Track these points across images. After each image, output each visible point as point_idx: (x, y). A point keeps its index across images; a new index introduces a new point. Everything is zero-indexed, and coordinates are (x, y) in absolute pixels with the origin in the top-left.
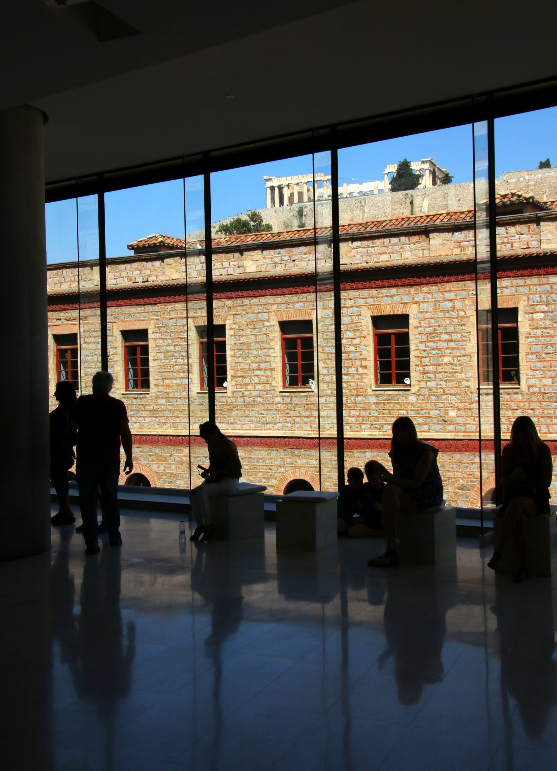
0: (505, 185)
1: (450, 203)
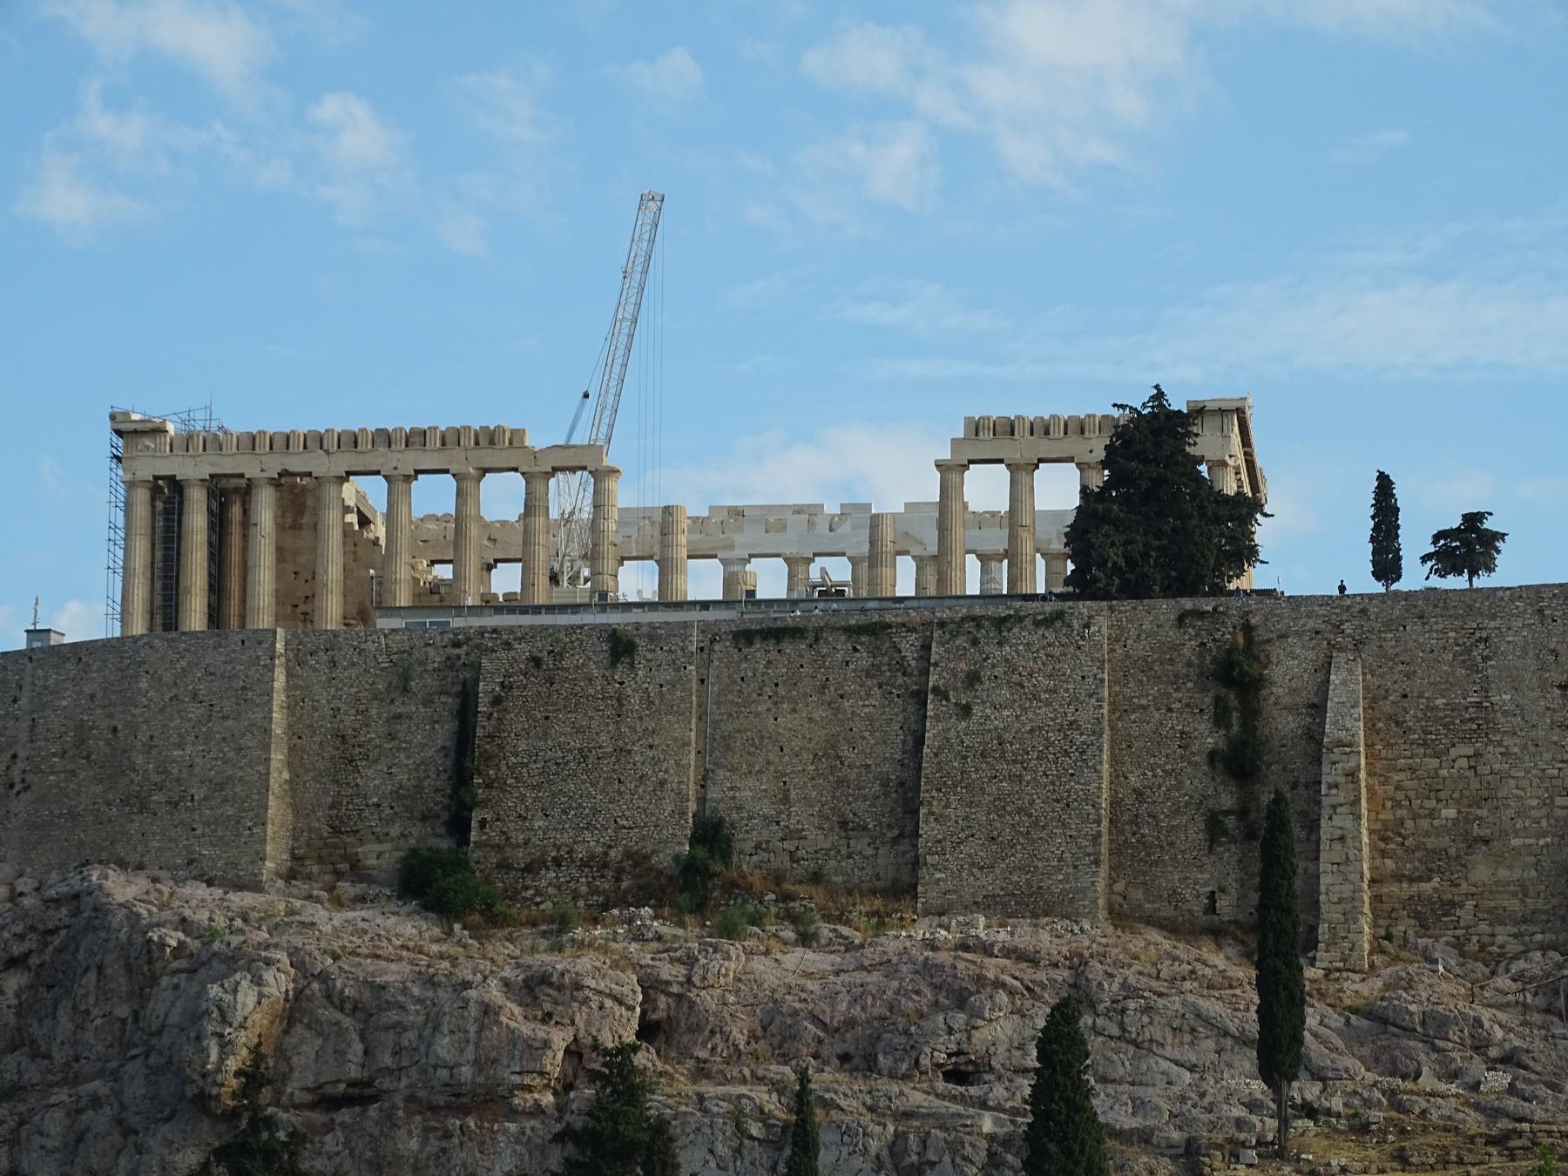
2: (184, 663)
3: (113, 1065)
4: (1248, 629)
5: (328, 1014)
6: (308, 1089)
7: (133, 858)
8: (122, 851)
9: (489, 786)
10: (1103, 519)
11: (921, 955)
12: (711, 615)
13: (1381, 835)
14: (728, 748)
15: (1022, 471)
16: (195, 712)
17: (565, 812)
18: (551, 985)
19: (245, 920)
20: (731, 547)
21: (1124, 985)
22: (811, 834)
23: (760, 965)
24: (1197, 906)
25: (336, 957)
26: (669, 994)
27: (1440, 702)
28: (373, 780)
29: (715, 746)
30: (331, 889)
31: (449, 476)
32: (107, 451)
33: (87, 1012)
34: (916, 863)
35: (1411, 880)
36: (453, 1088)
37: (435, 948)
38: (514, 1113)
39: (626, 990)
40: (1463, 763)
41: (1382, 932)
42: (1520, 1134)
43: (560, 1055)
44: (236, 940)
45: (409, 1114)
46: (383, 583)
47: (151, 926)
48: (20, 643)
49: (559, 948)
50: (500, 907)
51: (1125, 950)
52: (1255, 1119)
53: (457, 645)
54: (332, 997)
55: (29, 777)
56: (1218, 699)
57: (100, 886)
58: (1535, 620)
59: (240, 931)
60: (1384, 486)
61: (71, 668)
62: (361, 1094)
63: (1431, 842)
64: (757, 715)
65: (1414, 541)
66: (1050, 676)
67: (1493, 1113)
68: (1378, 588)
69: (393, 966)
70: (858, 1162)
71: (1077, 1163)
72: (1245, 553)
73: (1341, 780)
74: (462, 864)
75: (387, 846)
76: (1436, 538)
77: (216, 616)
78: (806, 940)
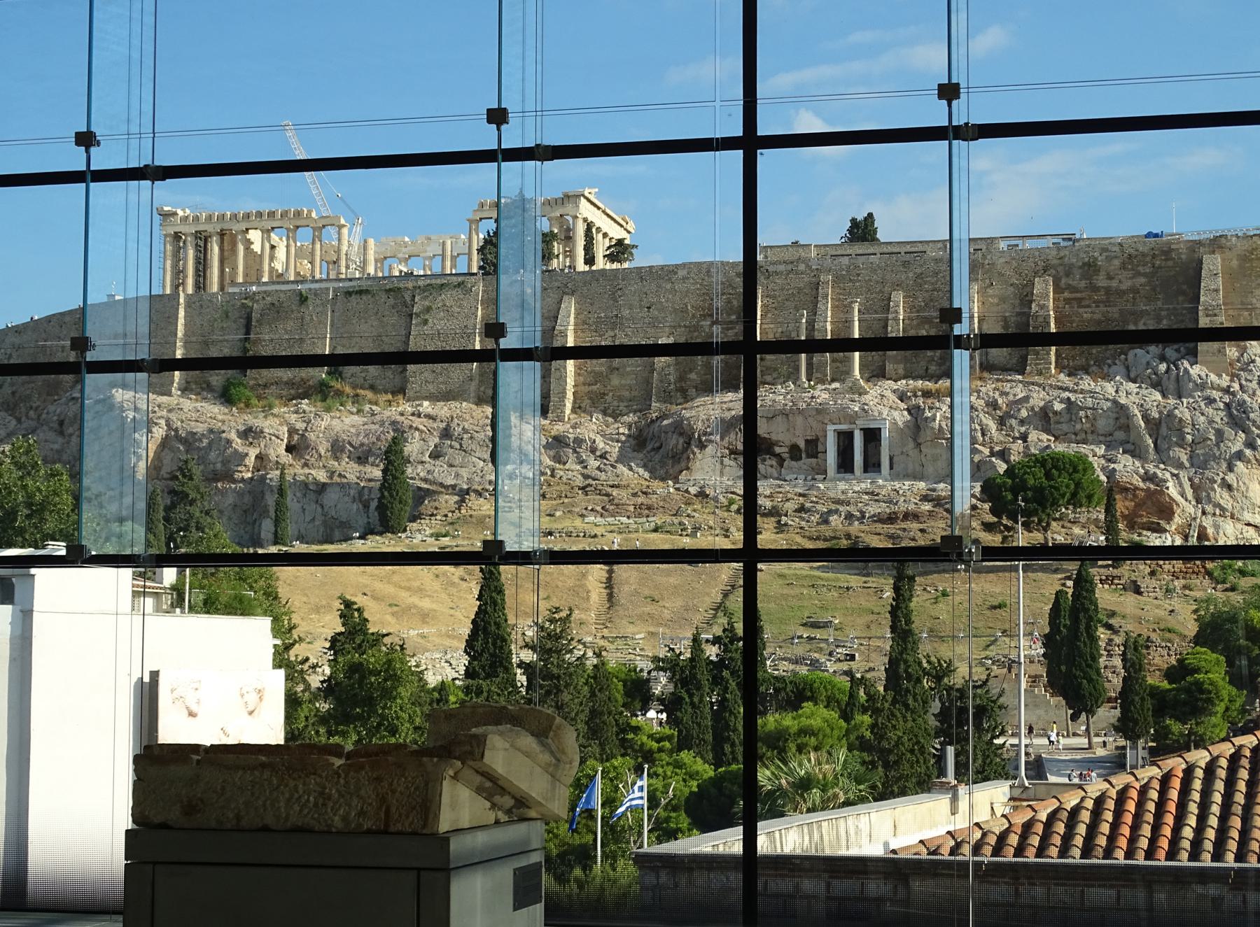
1: (626, 312)
12: (336, 285)
19: (159, 406)
23: (335, 422)
25: (182, 422)
35: (589, 385)
36: (215, 472)
37: (220, 417)
38: (234, 481)
39: (281, 433)
43: (253, 458)
46: (259, 272)
48: (105, 299)
53: (246, 299)
54: (177, 436)
59: (155, 412)
66: (459, 307)
67: (586, 477)
68: (587, 268)
70: (346, 499)
78: (359, 411)
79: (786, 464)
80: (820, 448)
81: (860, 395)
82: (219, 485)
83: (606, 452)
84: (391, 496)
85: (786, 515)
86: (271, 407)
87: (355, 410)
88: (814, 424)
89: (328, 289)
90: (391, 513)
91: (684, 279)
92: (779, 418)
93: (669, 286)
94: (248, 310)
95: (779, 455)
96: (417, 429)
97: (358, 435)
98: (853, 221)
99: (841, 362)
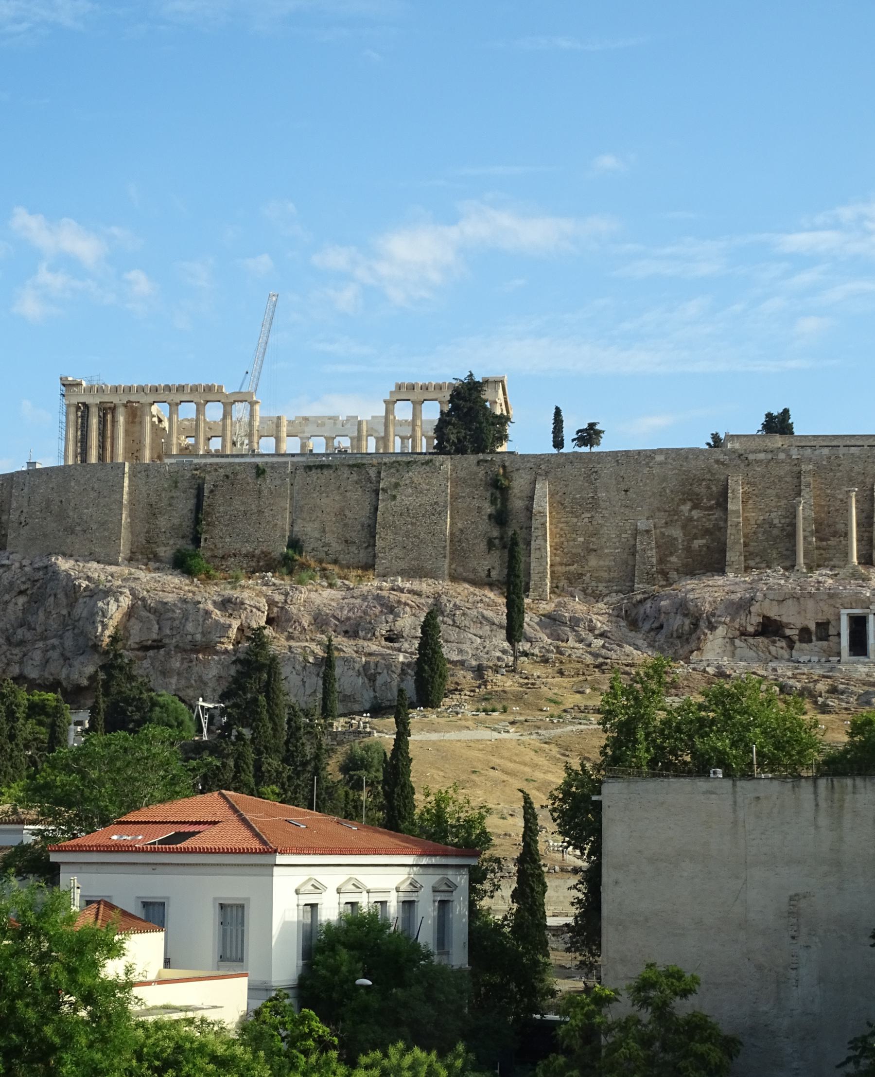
0: (742, 466)
1: (602, 495)
2: (88, 476)
3: (60, 633)
4: (504, 467)
5: (145, 614)
6: (137, 643)
7: (69, 552)
8: (63, 549)
9: (208, 525)
10: (449, 423)
11: (376, 592)
12: (295, 459)
13: (554, 548)
14: (302, 511)
15: (417, 405)
16: (93, 495)
17: (238, 535)
18: (232, 603)
19: (112, 577)
20: (304, 432)
21: (455, 605)
22: (334, 544)
23: (313, 595)
24: (483, 574)
25: (148, 591)
26: (278, 607)
27: (578, 496)
28: (162, 522)
29: (296, 510)
30: (146, 565)
31: (193, 404)
32: (59, 392)
33: (50, 612)
34: (375, 556)
35: (566, 565)
36: (194, 643)
37: (187, 588)
38: (217, 653)
39: (261, 605)
40: (586, 520)
41: (554, 585)
42: (607, 664)
43: (235, 630)
44: (108, 584)
45: (176, 652)
46: (169, 444)
47: (75, 579)
48: (24, 469)
49: (234, 588)
50: (212, 572)
51: (456, 591)
52: (505, 657)
53: (196, 469)
55: (28, 520)
56: (492, 494)
57: (55, 563)
58: (615, 464)
59: (110, 581)
60: (558, 412)
61: (44, 478)
62: (157, 645)
63: (574, 551)
64: (313, 498)
65: (569, 433)
66: (428, 484)
67: (596, 656)
68: (555, 451)
69: (170, 595)
70: (351, 672)
71: (436, 673)
72: (502, 437)
73: (539, 526)
74: (197, 555)
75: (168, 548)
76: (578, 432)
77: (101, 457)
78: (331, 586)
79: (797, 645)
80: (832, 631)
81: (863, 580)
82: (200, 656)
83: (605, 631)
84: (432, 670)
85: (821, 696)
86: (237, 579)
87: (325, 584)
88: (825, 608)
89: (286, 463)
90: (432, 687)
91: (660, 464)
92: (790, 602)
93: (646, 470)
94: (200, 481)
95: (788, 637)
96: (406, 604)
97: (342, 609)
98: (769, 416)
99: (824, 549)
